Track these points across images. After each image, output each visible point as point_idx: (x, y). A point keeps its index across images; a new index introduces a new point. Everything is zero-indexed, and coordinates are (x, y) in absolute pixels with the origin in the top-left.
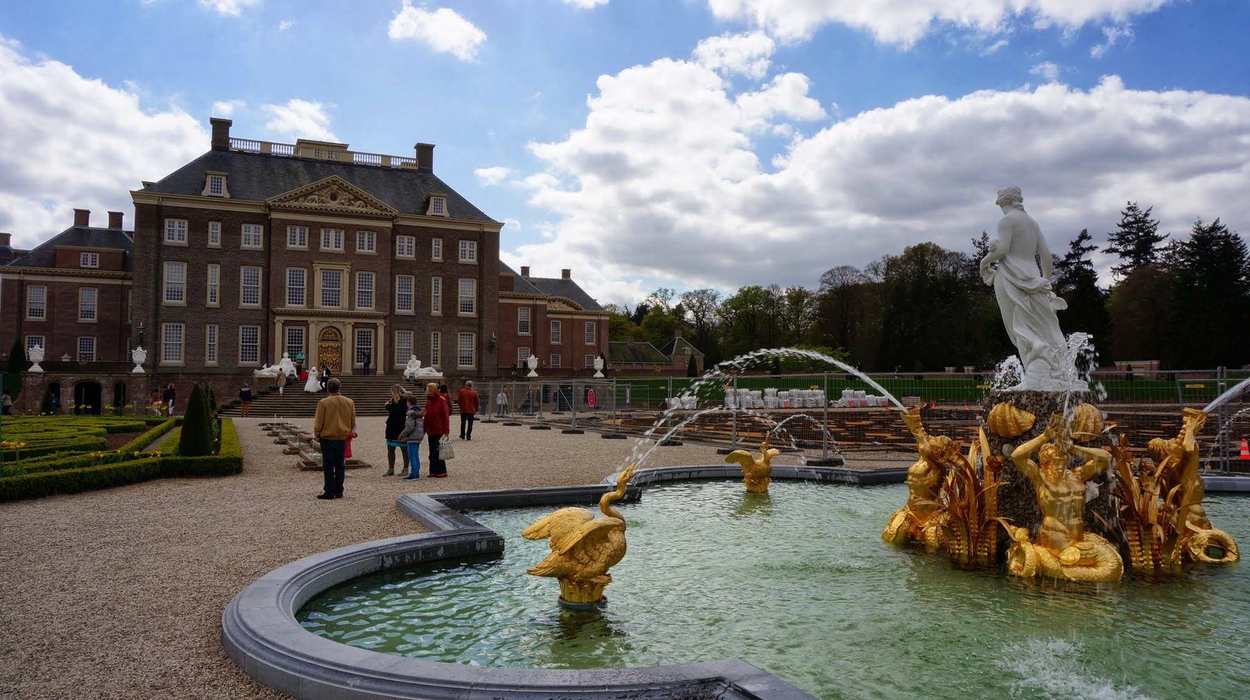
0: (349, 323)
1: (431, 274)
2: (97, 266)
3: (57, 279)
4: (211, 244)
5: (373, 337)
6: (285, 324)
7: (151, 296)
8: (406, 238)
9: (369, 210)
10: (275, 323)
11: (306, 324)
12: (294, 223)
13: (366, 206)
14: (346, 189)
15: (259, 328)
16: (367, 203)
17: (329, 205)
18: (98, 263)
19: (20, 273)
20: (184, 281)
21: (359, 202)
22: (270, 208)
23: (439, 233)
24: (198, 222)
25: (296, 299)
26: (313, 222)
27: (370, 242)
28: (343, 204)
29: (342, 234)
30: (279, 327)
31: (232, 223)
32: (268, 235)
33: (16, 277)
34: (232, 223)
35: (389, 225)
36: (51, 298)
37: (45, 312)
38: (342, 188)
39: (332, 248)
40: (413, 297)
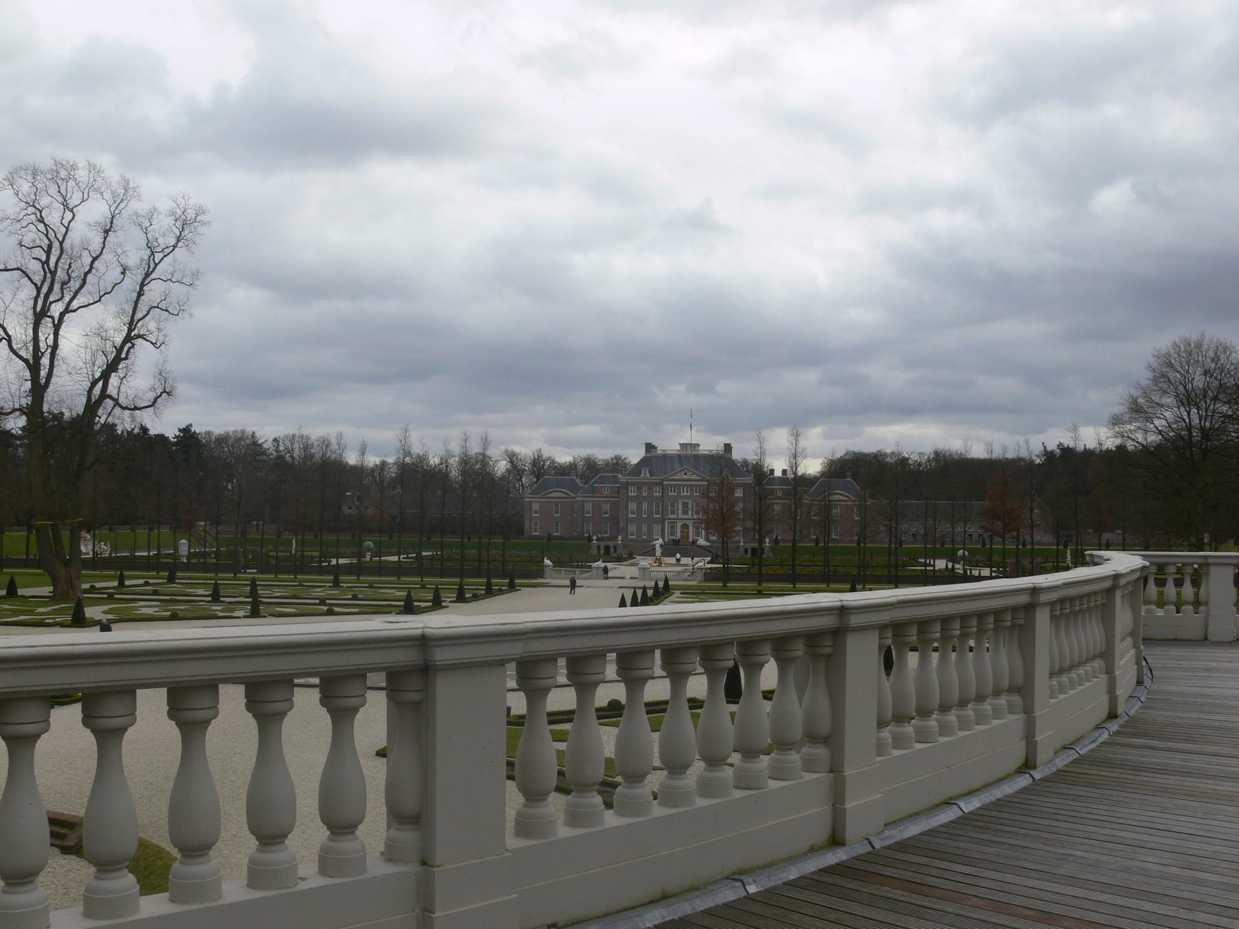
3: (596, 499)
4: (644, 494)
9: (698, 478)
12: (671, 485)
16: (698, 475)
24: (639, 486)
25: (673, 512)
31: (650, 486)
32: (663, 489)
33: (581, 499)
38: (688, 470)
39: (685, 494)
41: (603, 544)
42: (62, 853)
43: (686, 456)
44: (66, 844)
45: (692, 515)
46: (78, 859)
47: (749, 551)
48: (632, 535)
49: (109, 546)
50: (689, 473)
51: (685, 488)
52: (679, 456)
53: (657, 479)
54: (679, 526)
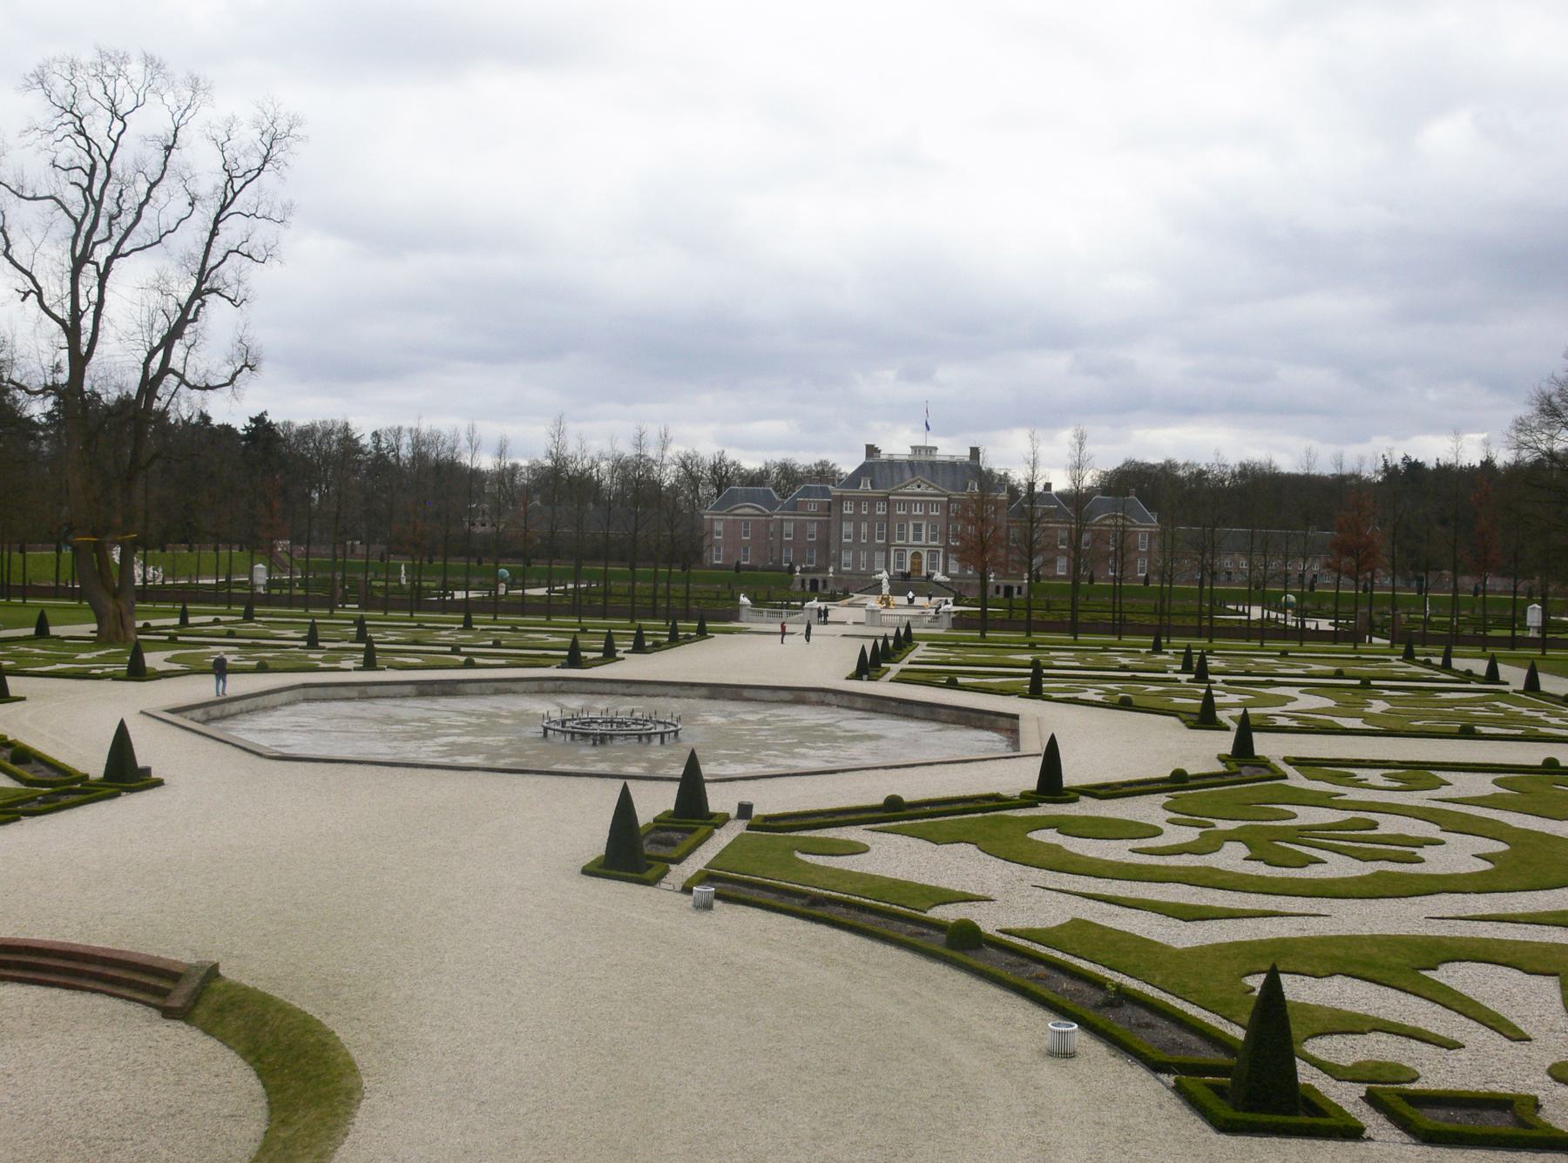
3: (798, 518)
4: (864, 512)
6: (896, 550)
11: (905, 551)
12: (900, 501)
16: (935, 488)
22: (889, 494)
24: (858, 502)
30: (892, 553)
31: (872, 501)
32: (888, 506)
33: (779, 517)
35: (946, 499)
39: (918, 513)
41: (809, 577)
42: (163, 1017)
43: (920, 464)
44: (168, 1004)
45: (927, 542)
46: (187, 1027)
47: (1002, 590)
48: (845, 566)
49: (160, 570)
50: (923, 486)
52: (911, 464)
53: (880, 492)
54: (909, 554)
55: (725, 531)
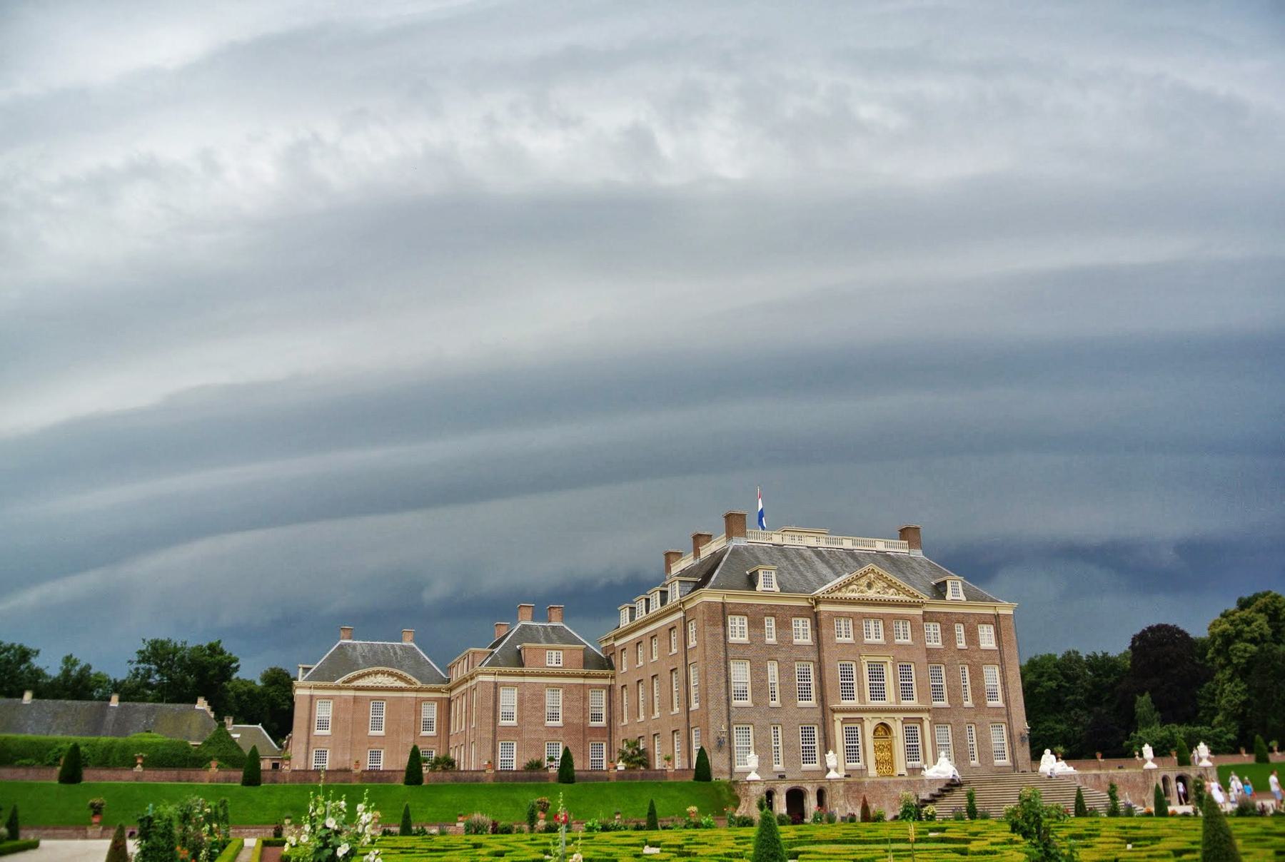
0: (899, 719)
1: (959, 662)
2: (561, 665)
5: (919, 733)
7: (724, 697)
8: (931, 624)
9: (902, 597)
10: (834, 721)
12: (839, 615)
13: (899, 594)
14: (880, 577)
15: (816, 728)
16: (899, 590)
17: (868, 594)
18: (561, 661)
19: (495, 674)
20: (749, 680)
21: (892, 590)
22: (818, 601)
23: (962, 619)
26: (856, 613)
27: (877, 630)
28: (879, 592)
29: (881, 623)
30: (838, 725)
32: (817, 626)
33: (491, 679)
34: (784, 618)
36: (521, 702)
37: (515, 715)
39: (872, 640)
40: (945, 688)
45: (898, 702)
51: (872, 623)
54: (869, 727)
55: (335, 718)
